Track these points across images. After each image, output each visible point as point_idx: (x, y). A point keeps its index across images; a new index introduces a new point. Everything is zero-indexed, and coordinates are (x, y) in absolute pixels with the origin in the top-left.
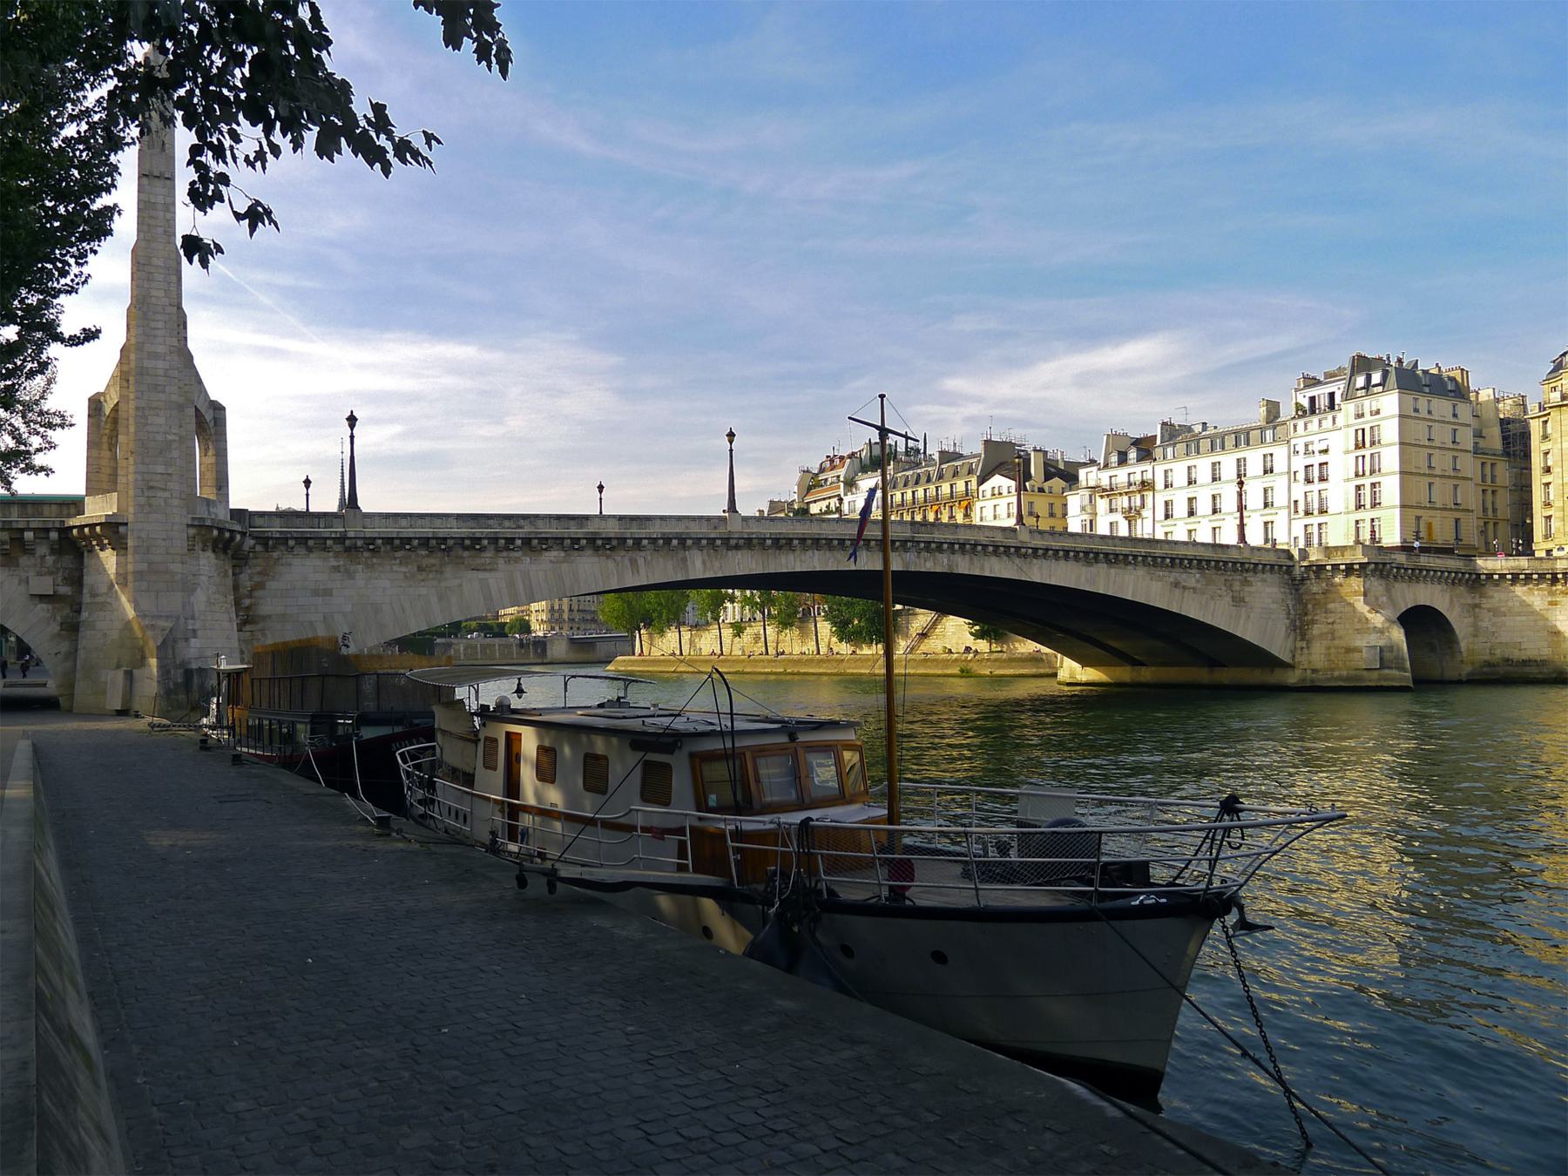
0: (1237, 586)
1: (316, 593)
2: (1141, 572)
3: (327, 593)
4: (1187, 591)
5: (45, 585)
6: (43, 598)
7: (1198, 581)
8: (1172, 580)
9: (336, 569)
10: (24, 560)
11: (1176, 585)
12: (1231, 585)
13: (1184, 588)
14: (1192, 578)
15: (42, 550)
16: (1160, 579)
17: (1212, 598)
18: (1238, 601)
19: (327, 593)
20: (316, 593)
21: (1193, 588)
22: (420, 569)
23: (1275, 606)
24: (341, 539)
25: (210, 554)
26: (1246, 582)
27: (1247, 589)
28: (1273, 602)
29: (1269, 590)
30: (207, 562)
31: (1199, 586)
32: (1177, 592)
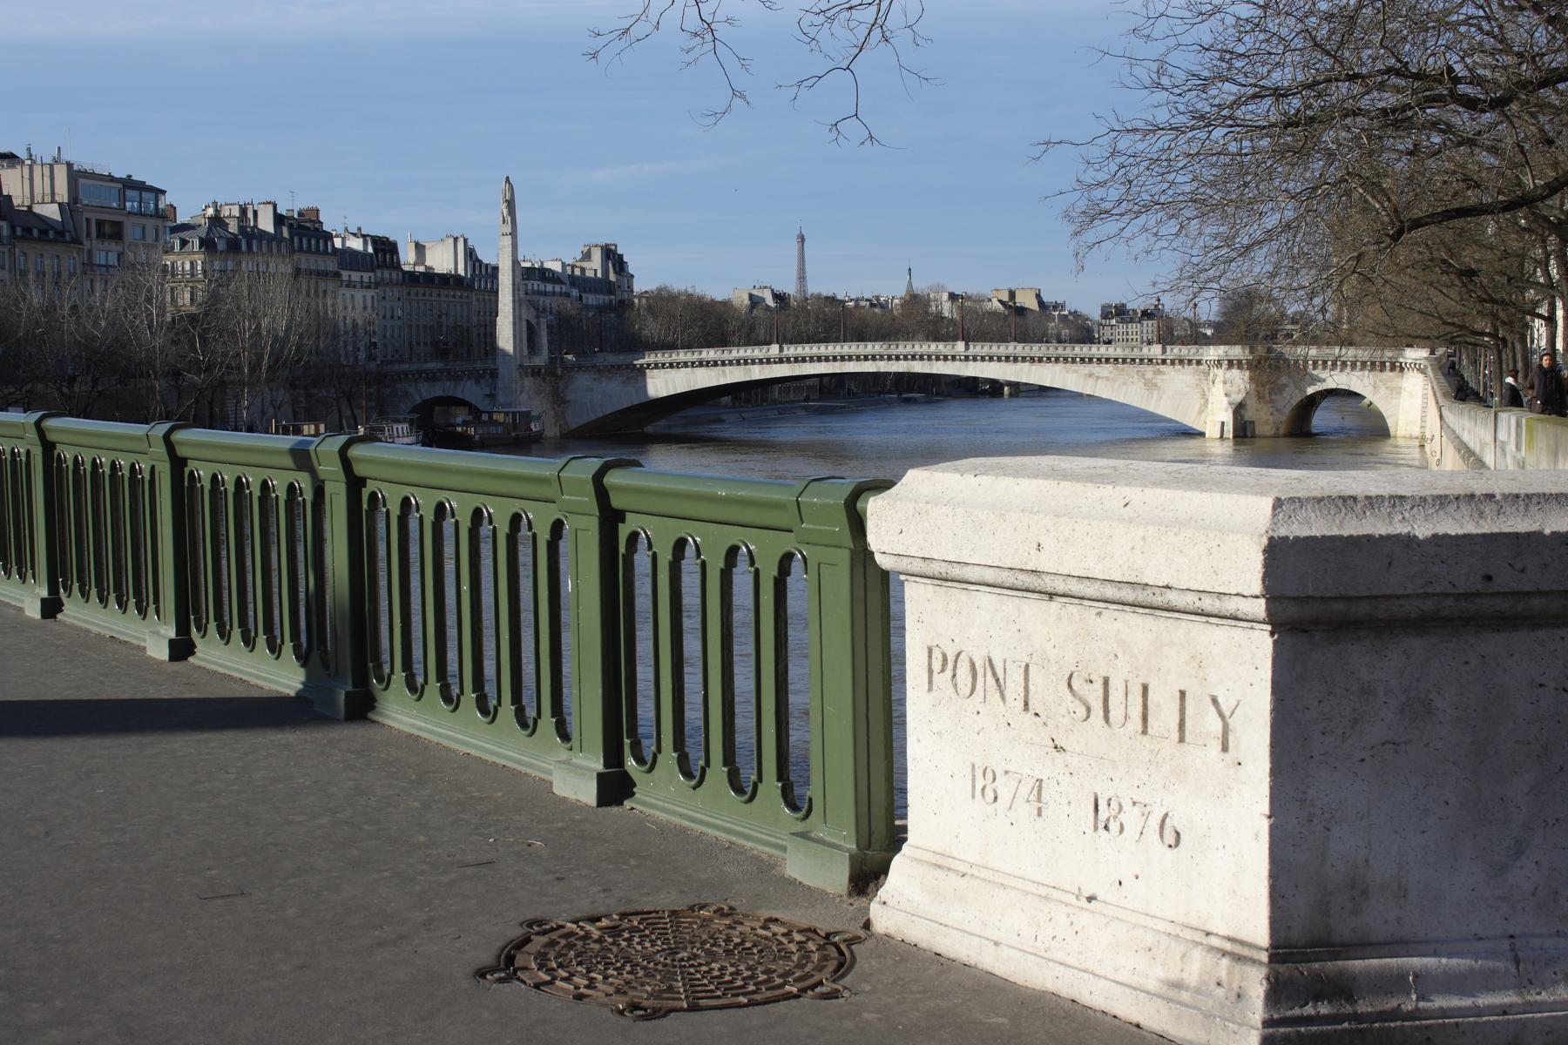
0: (1149, 375)
1: (587, 390)
2: (1059, 367)
3: (591, 390)
4: (1100, 381)
5: (487, 390)
6: (487, 395)
7: (1111, 372)
8: (1086, 372)
9: (595, 380)
10: (482, 381)
11: (1091, 375)
12: (1143, 375)
13: (1098, 378)
14: (1106, 370)
15: (487, 377)
16: (1075, 372)
17: (1124, 384)
18: (1151, 386)
19: (591, 390)
20: (587, 390)
21: (1107, 379)
22: (628, 378)
23: (1189, 389)
24: (594, 366)
25: (531, 378)
26: (1164, 373)
27: (1159, 377)
28: (1188, 386)
29: (1181, 377)
30: (529, 382)
31: (1112, 376)
32: (1091, 381)
